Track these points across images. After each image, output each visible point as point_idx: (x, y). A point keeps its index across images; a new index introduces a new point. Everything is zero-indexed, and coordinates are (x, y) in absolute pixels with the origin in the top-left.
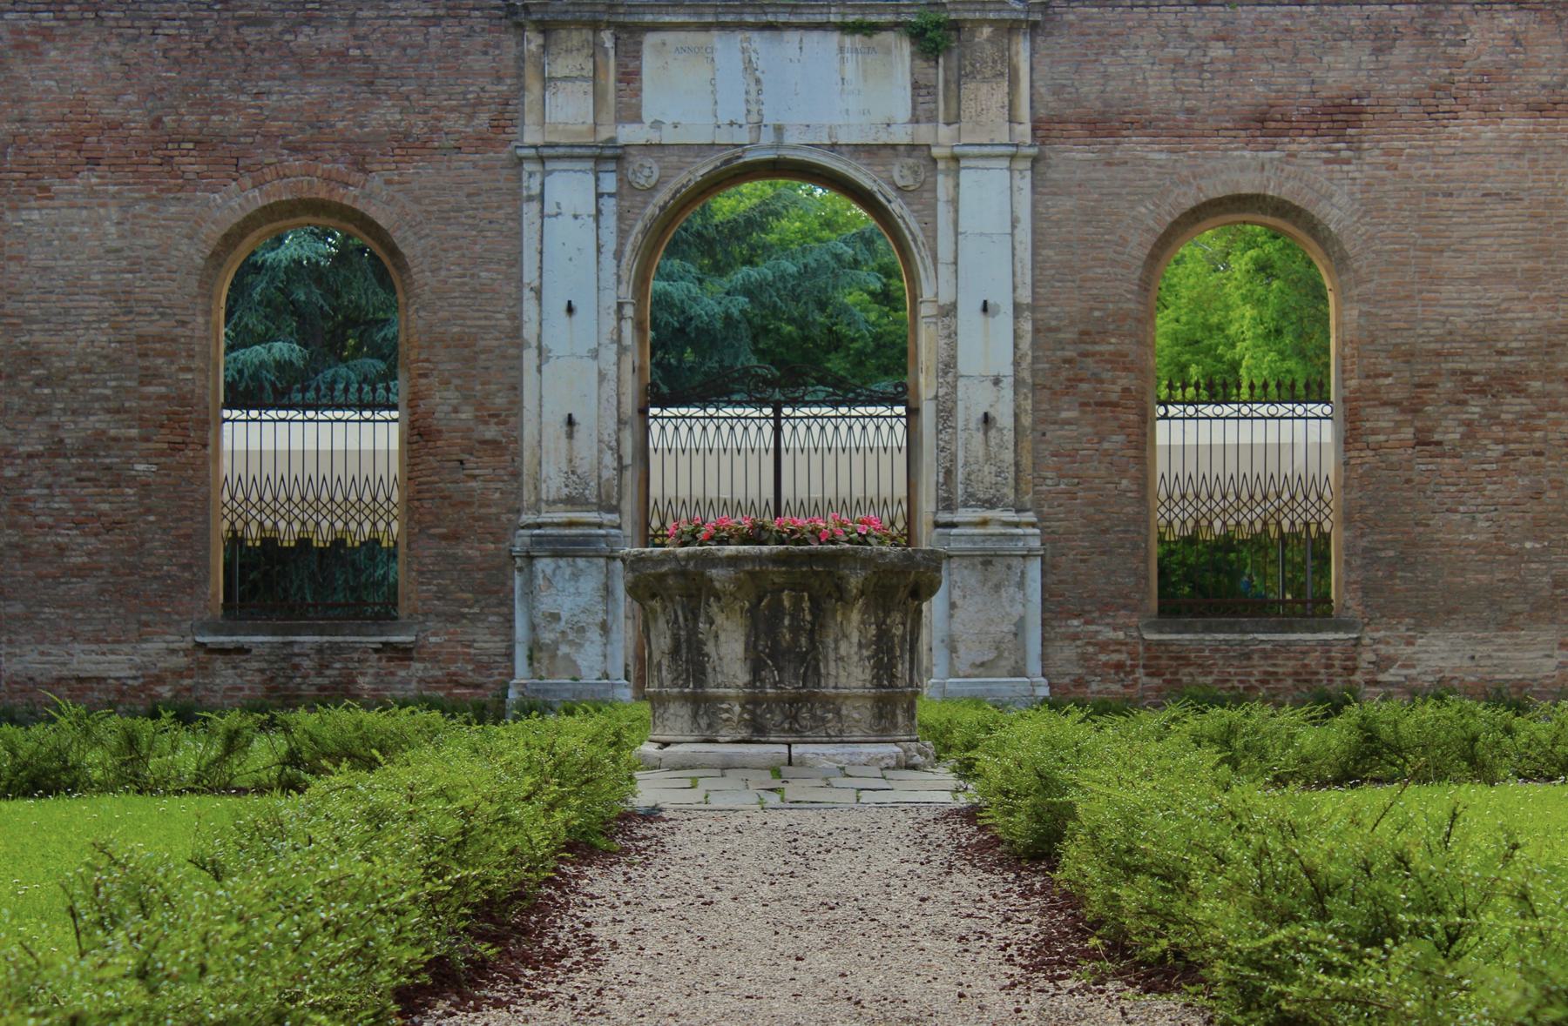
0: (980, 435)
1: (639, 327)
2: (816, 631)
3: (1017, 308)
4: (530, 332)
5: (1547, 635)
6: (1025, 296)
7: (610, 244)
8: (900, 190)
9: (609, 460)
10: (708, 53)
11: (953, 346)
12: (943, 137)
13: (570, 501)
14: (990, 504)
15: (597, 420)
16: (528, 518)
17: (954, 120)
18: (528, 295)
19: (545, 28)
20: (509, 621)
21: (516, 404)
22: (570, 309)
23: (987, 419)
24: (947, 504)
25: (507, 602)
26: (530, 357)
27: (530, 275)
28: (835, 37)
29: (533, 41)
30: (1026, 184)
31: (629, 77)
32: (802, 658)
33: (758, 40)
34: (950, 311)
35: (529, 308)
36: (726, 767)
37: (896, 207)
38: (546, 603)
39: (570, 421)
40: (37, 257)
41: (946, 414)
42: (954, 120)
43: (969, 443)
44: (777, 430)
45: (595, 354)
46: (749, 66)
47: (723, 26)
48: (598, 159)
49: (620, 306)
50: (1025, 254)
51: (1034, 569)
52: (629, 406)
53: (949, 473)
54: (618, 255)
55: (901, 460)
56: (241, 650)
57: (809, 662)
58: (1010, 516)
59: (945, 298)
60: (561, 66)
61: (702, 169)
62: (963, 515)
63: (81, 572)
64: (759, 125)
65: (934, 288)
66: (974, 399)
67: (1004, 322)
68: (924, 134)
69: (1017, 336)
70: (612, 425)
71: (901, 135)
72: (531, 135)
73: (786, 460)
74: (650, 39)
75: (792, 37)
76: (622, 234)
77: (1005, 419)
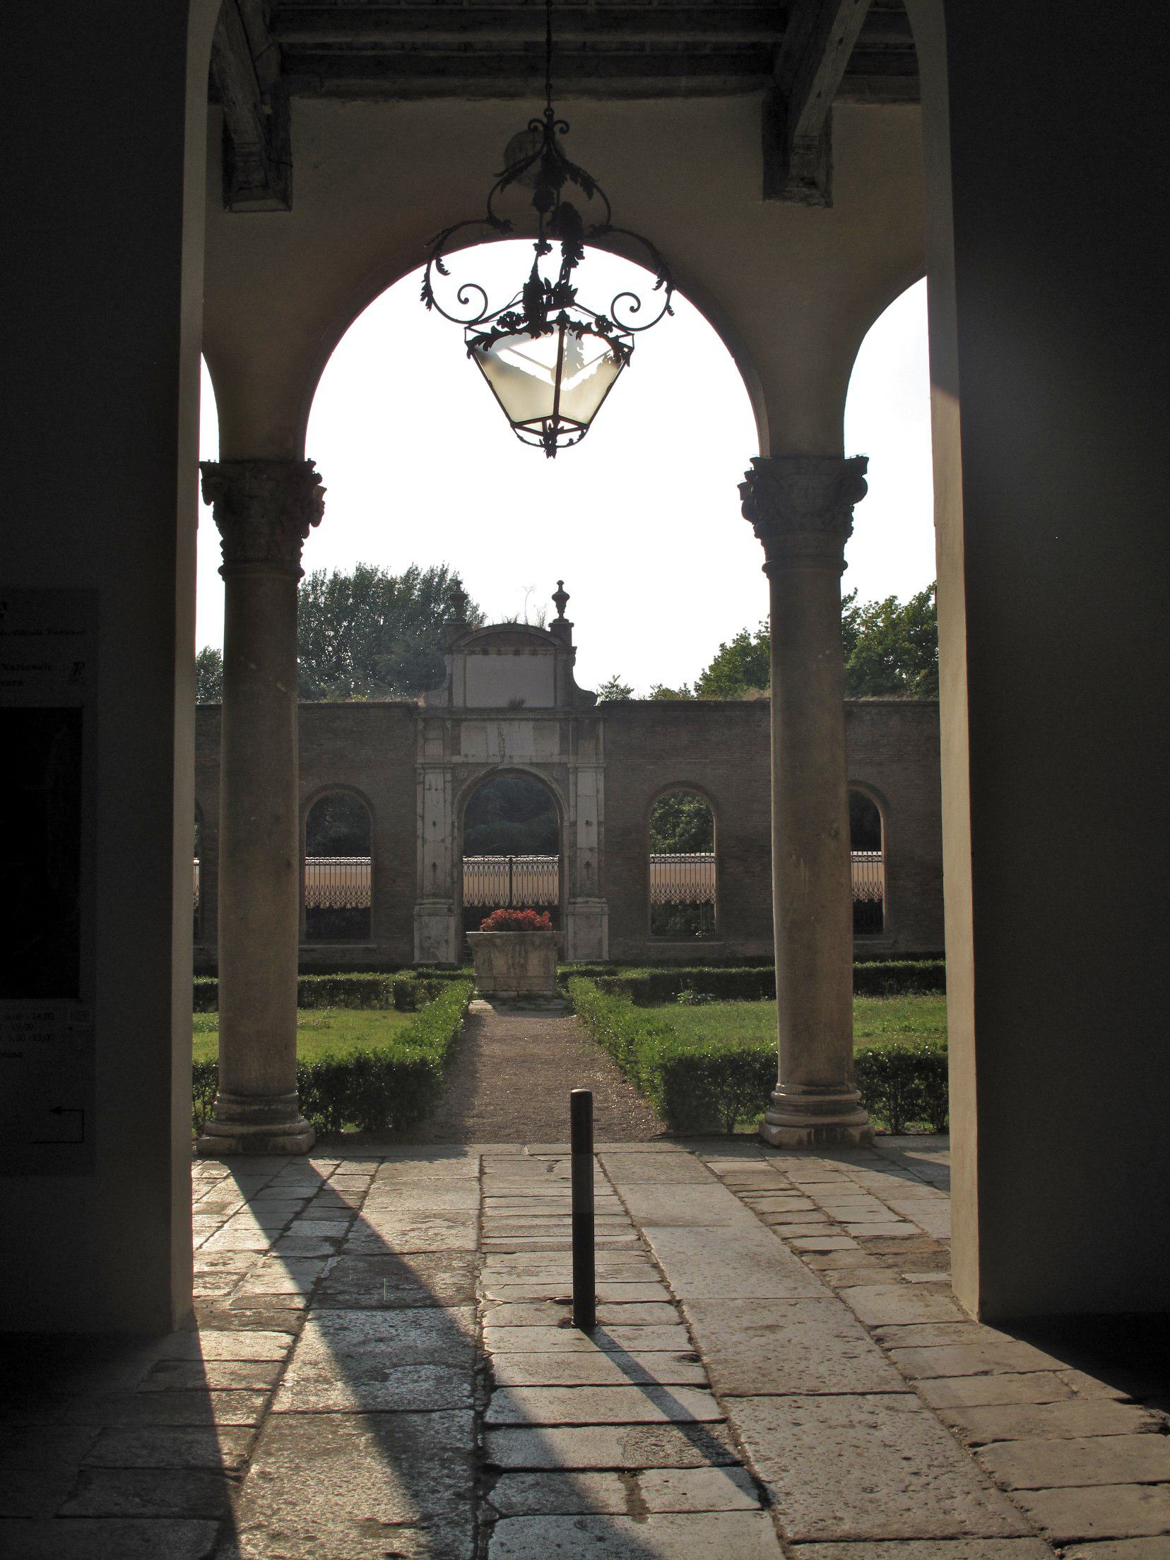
0: (585, 871)
1: (459, 828)
2: (526, 958)
3: (599, 823)
4: (419, 833)
6: (602, 818)
7: (449, 798)
8: (557, 780)
9: (448, 879)
11: (575, 837)
12: (571, 760)
13: (435, 895)
14: (589, 895)
16: (419, 901)
17: (576, 754)
18: (419, 819)
21: (415, 860)
22: (434, 824)
23: (588, 865)
24: (573, 895)
25: (411, 932)
26: (419, 842)
27: (419, 810)
28: (531, 724)
32: (522, 966)
33: (503, 724)
34: (574, 824)
35: (419, 823)
37: (554, 786)
39: (434, 865)
41: (573, 862)
42: (576, 754)
44: (511, 868)
45: (443, 841)
46: (500, 734)
47: (490, 719)
48: (444, 768)
49: (453, 823)
50: (602, 804)
51: (606, 919)
52: (455, 857)
53: (574, 884)
54: (452, 804)
55: (556, 878)
56: (313, 950)
58: (597, 900)
59: (572, 819)
60: (431, 734)
62: (579, 900)
64: (503, 756)
65: (569, 816)
66: (585, 857)
67: (594, 828)
68: (565, 759)
69: (599, 834)
70: (449, 865)
71: (556, 759)
72: (420, 760)
73: (514, 879)
74: (464, 724)
75: (516, 723)
76: (454, 796)
77: (595, 863)
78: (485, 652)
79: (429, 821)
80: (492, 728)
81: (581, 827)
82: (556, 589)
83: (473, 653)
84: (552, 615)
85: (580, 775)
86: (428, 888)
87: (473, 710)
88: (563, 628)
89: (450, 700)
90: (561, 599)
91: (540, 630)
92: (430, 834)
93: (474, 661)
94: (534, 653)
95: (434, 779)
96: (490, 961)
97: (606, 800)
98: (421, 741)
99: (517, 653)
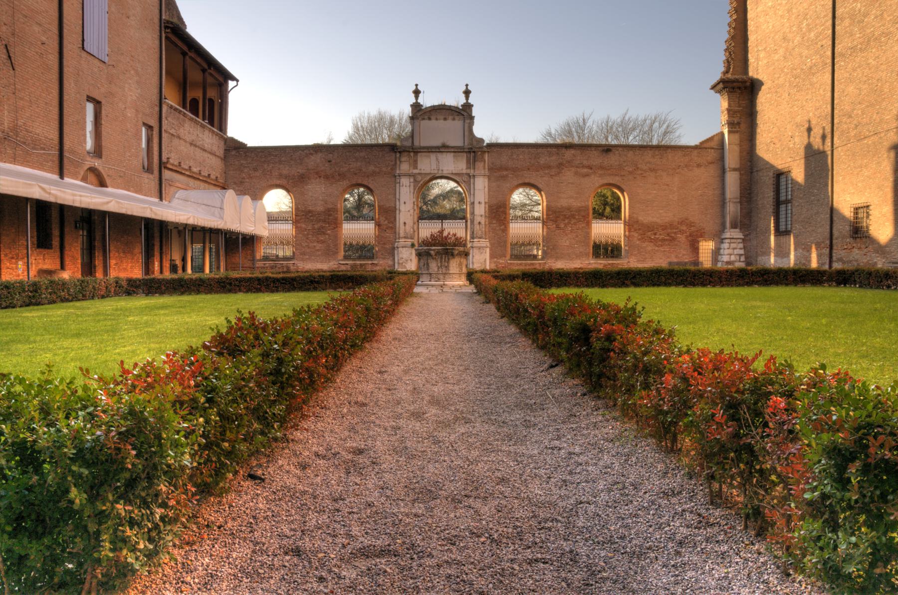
5: (579, 261)
10: (429, 157)
12: (472, 172)
13: (405, 237)
15: (410, 223)
19: (400, 152)
20: (394, 259)
23: (479, 223)
24: (472, 238)
25: (393, 255)
29: (398, 155)
30: (486, 180)
31: (416, 162)
33: (439, 155)
34: (473, 203)
36: (433, 286)
38: (401, 256)
40: (310, 194)
41: (472, 222)
43: (477, 227)
46: (437, 159)
51: (488, 250)
52: (416, 220)
57: (447, 267)
60: (403, 159)
61: (428, 178)
63: (318, 250)
66: (478, 219)
67: (483, 205)
68: (468, 171)
71: (464, 171)
74: (419, 154)
77: (483, 222)
78: (430, 119)
79: (402, 201)
80: (433, 156)
81: (477, 206)
82: (464, 88)
83: (424, 119)
84: (462, 100)
85: (476, 179)
86: (402, 234)
87: (424, 148)
88: (468, 107)
89: (413, 142)
90: (467, 93)
91: (457, 108)
92: (403, 207)
93: (425, 123)
94: (454, 119)
95: (405, 181)
96: (428, 264)
97: (489, 190)
98: (398, 162)
99: (445, 119)
